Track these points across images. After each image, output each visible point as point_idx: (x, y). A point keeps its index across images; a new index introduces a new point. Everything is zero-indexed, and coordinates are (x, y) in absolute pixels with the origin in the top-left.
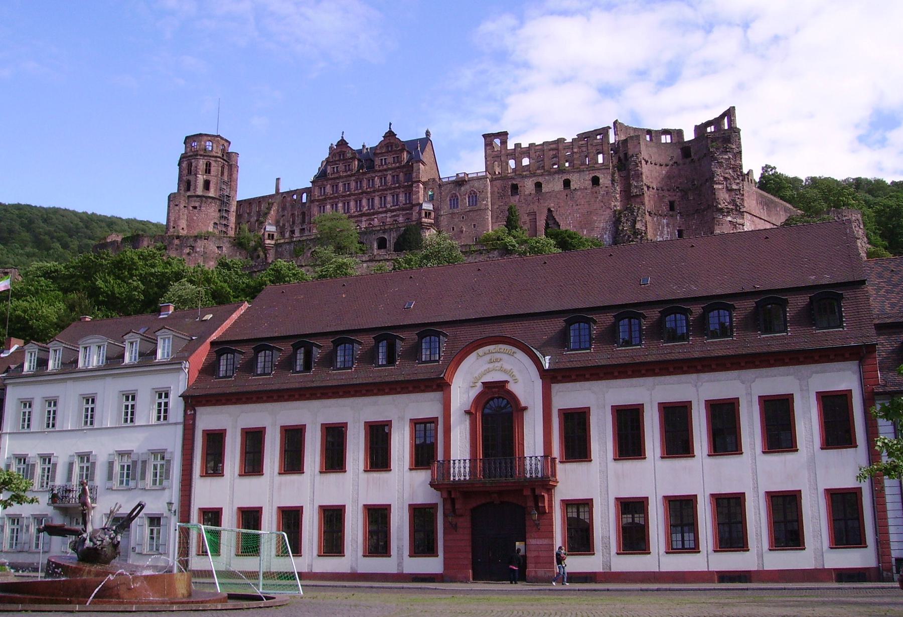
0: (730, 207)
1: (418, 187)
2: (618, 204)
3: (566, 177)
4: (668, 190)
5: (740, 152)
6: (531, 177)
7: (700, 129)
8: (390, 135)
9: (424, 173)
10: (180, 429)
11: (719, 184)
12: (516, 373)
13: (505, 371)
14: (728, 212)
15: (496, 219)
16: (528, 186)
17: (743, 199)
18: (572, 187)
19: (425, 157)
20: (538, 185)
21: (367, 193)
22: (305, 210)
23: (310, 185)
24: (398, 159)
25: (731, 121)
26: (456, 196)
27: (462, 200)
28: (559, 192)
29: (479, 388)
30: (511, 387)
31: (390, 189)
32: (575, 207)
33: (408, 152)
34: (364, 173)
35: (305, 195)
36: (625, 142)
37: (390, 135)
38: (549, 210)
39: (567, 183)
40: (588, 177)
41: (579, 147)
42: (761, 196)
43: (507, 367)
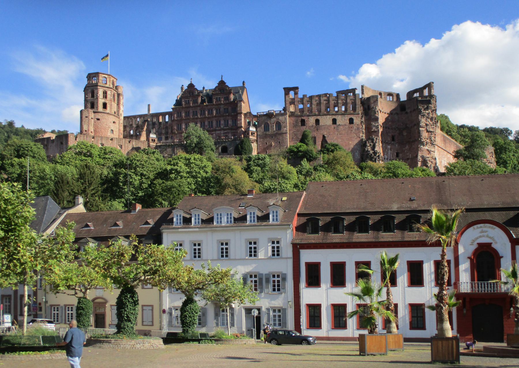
0: (428, 141)
1: (241, 117)
2: (364, 135)
3: (334, 117)
4: (392, 129)
5: (436, 110)
6: (313, 116)
7: (410, 94)
8: (222, 83)
9: (244, 108)
10: (290, 263)
11: (423, 127)
12: (496, 239)
13: (490, 238)
14: (426, 144)
15: (292, 139)
16: (311, 121)
17: (435, 137)
18: (338, 123)
19: (244, 97)
20: (317, 121)
21: (208, 118)
22: (168, 125)
23: (171, 110)
24: (228, 98)
25: (430, 91)
26: (268, 124)
27: (272, 127)
28: (330, 126)
29: (475, 246)
30: (493, 246)
31: (223, 116)
32: (339, 136)
33: (233, 94)
34: (207, 105)
35: (167, 117)
36: (369, 99)
37: (222, 83)
38: (324, 137)
39: (334, 121)
40: (347, 117)
41: (342, 100)
42: (444, 136)
43: (490, 235)
